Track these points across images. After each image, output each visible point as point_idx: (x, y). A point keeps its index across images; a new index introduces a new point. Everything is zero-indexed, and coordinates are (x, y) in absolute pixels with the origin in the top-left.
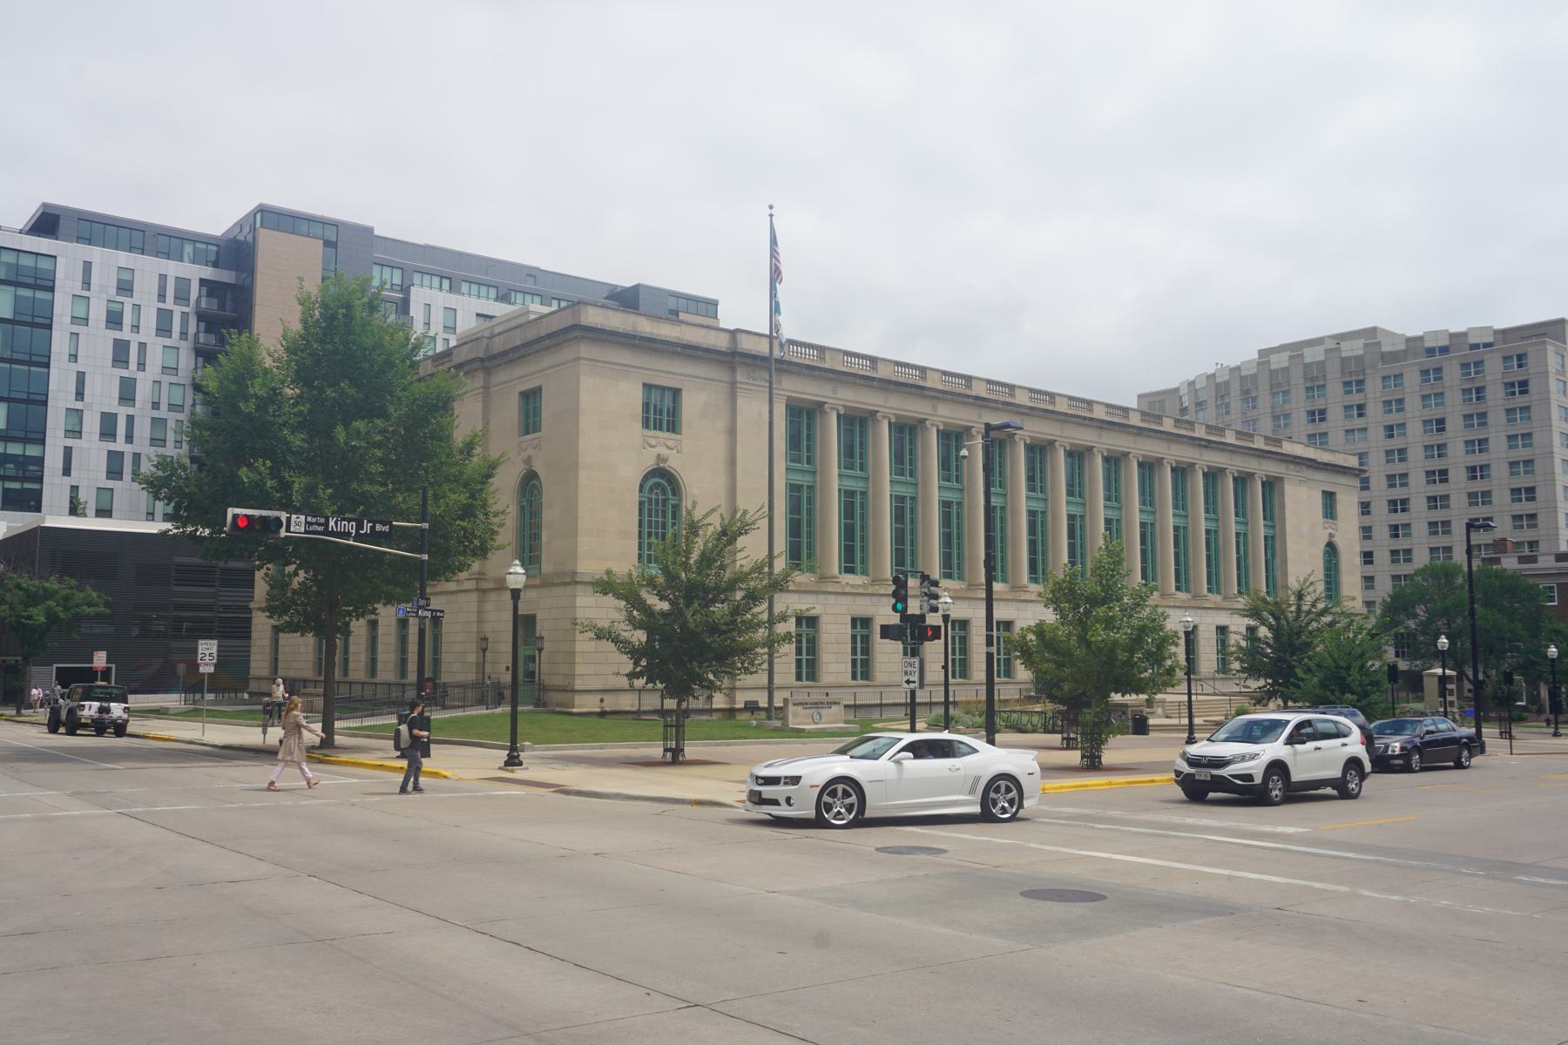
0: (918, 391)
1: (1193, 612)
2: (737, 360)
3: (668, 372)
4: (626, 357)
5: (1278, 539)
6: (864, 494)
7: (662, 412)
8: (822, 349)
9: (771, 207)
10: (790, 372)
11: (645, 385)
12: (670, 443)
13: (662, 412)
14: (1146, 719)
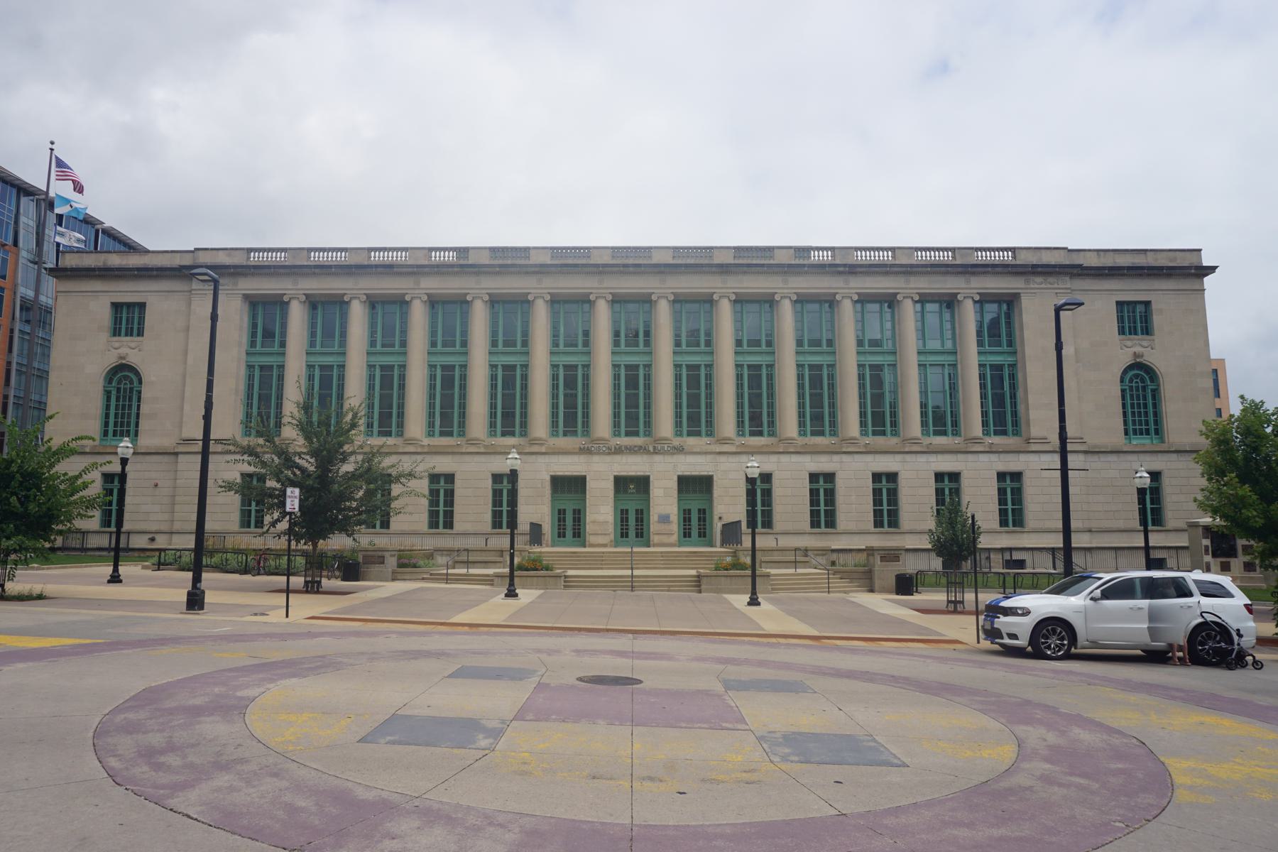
0: (388, 269)
1: (758, 457)
2: (182, 271)
3: (128, 292)
4: (97, 285)
5: (1019, 365)
6: (831, 366)
7: (128, 319)
8: (1013, 250)
9: (52, 143)
10: (245, 275)
11: (113, 304)
12: (133, 345)
13: (128, 319)
14: (945, 565)
